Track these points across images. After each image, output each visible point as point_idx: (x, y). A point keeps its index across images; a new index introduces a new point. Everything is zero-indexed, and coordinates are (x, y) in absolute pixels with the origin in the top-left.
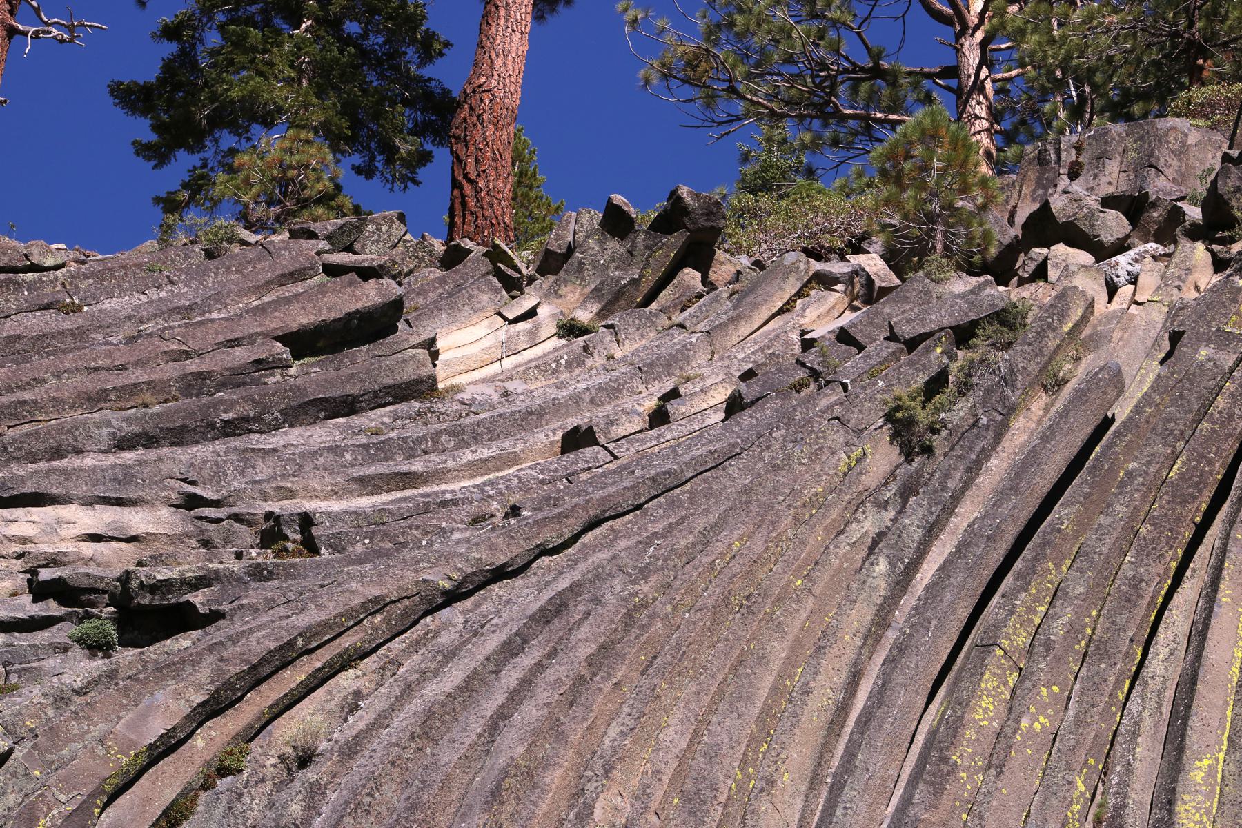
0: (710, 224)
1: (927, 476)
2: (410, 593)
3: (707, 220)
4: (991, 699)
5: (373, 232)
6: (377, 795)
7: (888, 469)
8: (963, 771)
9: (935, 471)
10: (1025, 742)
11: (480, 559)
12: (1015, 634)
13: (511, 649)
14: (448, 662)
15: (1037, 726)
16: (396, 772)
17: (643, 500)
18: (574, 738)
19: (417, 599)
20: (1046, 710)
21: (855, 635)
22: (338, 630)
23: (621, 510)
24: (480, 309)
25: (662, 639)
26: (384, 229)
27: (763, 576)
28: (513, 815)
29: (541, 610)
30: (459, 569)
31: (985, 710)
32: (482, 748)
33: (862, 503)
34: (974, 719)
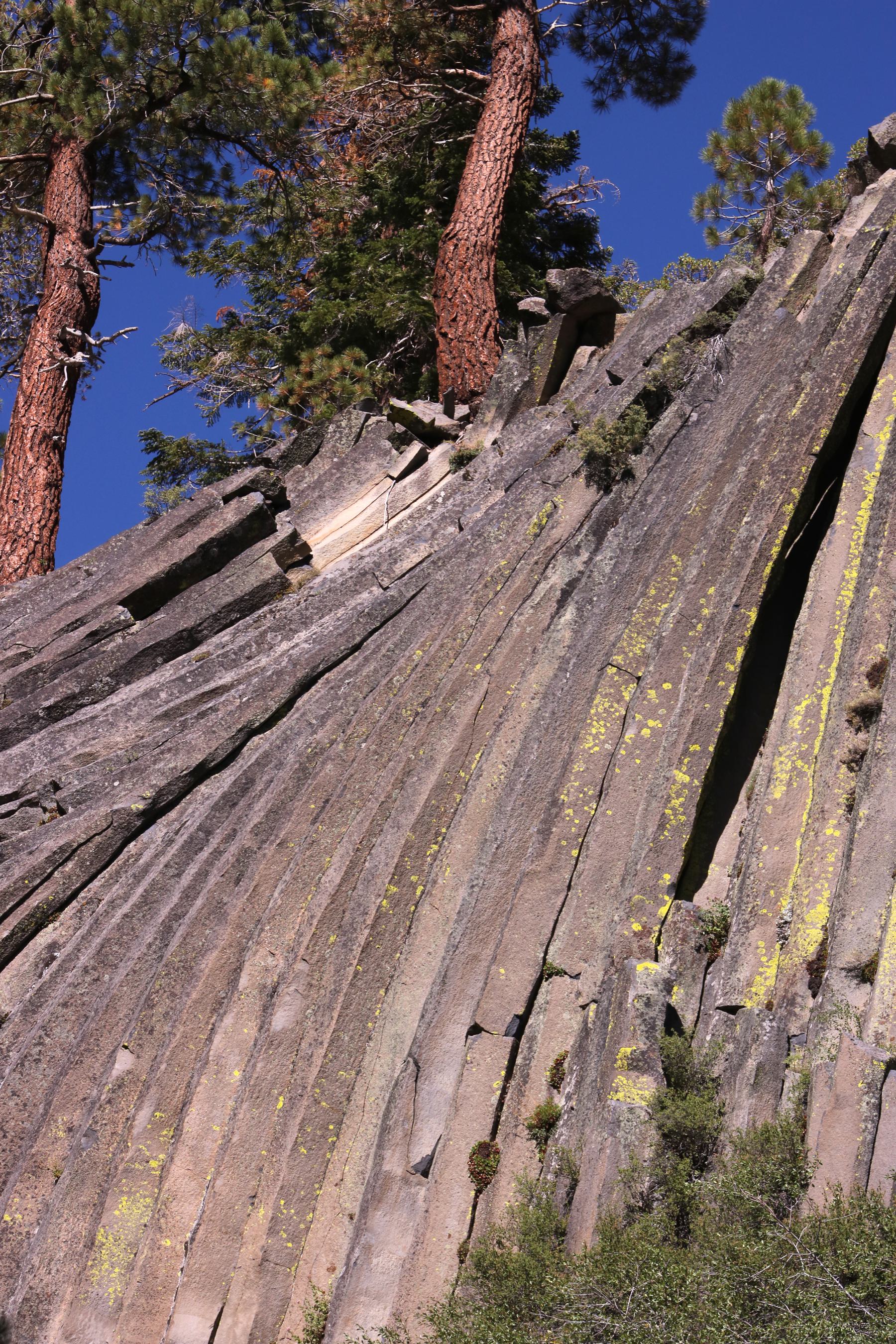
0: (582, 296)
1: (627, 501)
2: (99, 830)
3: (578, 294)
4: (602, 723)
5: (335, 432)
6: (47, 1040)
7: (583, 511)
8: (569, 808)
9: (637, 492)
10: (632, 753)
11: (175, 768)
12: (631, 644)
13: (193, 847)
14: (139, 882)
15: (646, 732)
16: (69, 1012)
17: (358, 639)
18: (233, 914)
19: (110, 831)
20: (656, 711)
21: (533, 699)
22: (22, 894)
23: (333, 659)
24: (368, 479)
25: (333, 781)
26: (344, 424)
27: (440, 675)
28: (167, 1013)
29: (224, 796)
30: (152, 786)
31: (596, 736)
32: (154, 956)
33: (553, 557)
34: (584, 750)
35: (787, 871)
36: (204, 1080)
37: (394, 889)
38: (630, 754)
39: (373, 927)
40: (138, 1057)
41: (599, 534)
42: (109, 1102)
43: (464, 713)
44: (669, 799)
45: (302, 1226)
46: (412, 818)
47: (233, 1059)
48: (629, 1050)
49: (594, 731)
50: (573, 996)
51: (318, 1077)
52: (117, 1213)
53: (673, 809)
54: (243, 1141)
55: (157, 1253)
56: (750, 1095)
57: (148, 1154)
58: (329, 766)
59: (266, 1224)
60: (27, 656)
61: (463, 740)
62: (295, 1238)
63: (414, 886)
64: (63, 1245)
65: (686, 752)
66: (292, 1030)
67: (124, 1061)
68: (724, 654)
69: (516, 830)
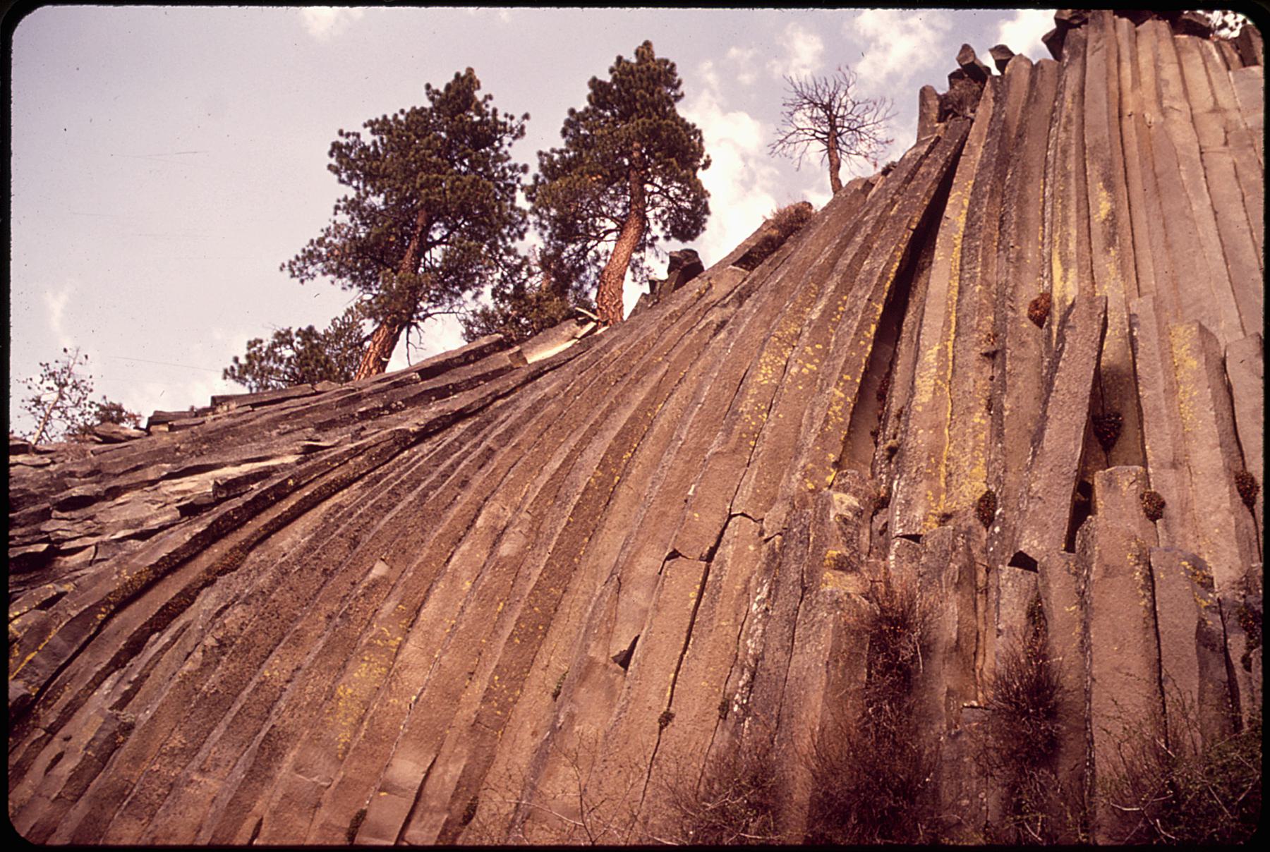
15: (805, 371)
31: (765, 375)
35: (942, 448)
36: (441, 585)
37: (600, 474)
38: (795, 382)
39: (583, 494)
40: (391, 567)
41: (741, 299)
42: (364, 595)
43: (652, 381)
44: (830, 405)
45: (511, 699)
46: (615, 433)
47: (465, 574)
48: (835, 553)
49: (763, 372)
50: (756, 534)
51: (534, 589)
52: (356, 675)
53: (834, 412)
54: (467, 630)
55: (385, 709)
56: (956, 592)
57: (388, 634)
58: (553, 406)
59: (481, 694)
60: (353, 391)
61: (650, 394)
62: (504, 707)
63: (613, 476)
64: (307, 696)
65: (841, 378)
66: (515, 558)
67: (379, 570)
68: (863, 326)
69: (695, 436)
